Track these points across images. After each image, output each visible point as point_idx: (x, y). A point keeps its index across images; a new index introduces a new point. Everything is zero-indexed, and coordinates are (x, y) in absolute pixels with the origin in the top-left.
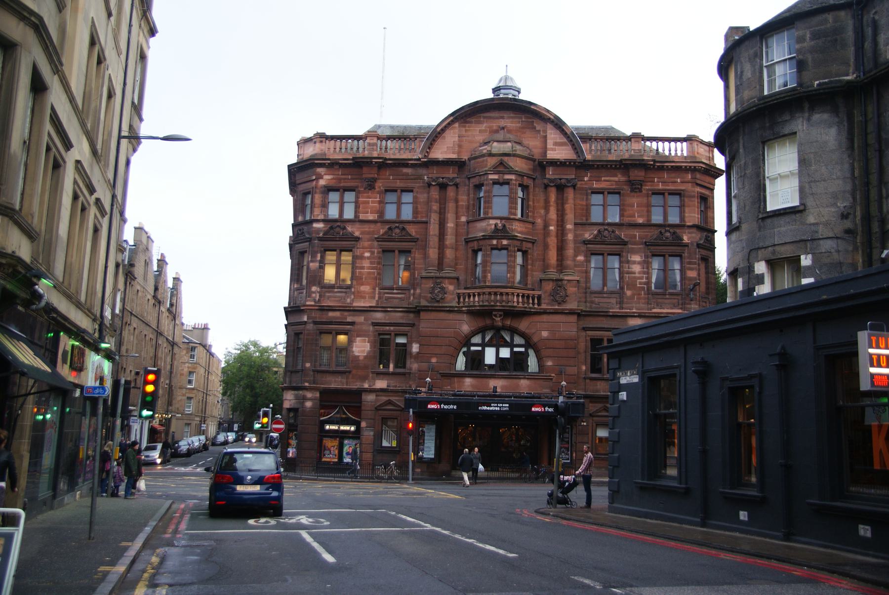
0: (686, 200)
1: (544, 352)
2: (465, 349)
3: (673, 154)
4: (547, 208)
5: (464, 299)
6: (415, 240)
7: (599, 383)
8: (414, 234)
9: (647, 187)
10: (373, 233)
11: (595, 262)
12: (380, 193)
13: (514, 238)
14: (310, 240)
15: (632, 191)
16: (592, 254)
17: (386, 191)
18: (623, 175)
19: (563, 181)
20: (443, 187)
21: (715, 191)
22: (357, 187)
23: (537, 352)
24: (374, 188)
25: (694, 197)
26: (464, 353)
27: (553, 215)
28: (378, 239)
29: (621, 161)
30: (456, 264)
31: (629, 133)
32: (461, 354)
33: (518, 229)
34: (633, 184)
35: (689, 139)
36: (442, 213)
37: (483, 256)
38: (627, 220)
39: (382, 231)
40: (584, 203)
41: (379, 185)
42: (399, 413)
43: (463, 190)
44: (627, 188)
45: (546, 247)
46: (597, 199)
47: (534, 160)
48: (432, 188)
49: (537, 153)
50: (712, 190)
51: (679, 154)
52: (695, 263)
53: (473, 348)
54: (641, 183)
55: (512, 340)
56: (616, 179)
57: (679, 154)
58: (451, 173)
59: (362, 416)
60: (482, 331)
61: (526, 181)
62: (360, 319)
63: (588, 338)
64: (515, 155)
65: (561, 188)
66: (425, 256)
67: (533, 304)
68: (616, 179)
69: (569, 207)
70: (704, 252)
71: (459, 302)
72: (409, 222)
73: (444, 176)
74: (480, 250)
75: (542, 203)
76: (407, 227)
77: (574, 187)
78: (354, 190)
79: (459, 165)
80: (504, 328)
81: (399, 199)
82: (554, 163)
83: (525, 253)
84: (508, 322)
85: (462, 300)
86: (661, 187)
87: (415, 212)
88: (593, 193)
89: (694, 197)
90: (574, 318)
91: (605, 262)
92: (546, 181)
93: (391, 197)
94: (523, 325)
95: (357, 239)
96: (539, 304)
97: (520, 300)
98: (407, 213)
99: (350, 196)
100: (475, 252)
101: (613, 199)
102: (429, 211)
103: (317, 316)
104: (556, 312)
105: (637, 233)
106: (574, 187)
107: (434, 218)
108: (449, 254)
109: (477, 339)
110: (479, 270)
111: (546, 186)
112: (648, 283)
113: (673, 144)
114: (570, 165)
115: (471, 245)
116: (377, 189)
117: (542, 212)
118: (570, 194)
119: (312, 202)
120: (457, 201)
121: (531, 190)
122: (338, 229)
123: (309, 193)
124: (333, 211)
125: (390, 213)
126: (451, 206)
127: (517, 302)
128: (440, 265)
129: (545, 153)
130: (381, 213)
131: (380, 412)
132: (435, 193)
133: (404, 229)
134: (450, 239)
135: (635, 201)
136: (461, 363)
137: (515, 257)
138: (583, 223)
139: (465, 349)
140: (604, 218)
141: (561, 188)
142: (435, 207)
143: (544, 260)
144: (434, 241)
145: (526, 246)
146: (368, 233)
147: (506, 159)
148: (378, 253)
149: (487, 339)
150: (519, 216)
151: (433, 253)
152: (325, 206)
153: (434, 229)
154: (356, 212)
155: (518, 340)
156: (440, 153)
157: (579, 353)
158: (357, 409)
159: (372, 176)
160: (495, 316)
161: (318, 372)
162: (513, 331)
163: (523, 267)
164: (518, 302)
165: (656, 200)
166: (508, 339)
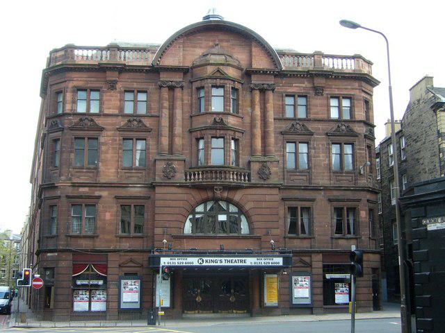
0: (356, 102)
1: (254, 218)
2: (191, 216)
3: (345, 68)
4: (252, 105)
5: (190, 176)
6: (149, 131)
7: (295, 241)
8: (148, 125)
9: (326, 92)
10: (115, 124)
11: (290, 148)
12: (120, 92)
13: (228, 129)
14: (62, 130)
15: (317, 94)
16: (287, 142)
17: (126, 91)
18: (309, 83)
19: (265, 86)
20: (172, 88)
21: (373, 97)
22: (102, 88)
23: (248, 218)
24: (116, 89)
25: (360, 100)
26: (190, 219)
27: (258, 112)
28: (118, 129)
29: (308, 71)
30: (183, 150)
31: (311, 52)
32: (188, 221)
33: (231, 121)
34: (317, 90)
36: (172, 109)
37: (205, 143)
38: (312, 116)
39: (122, 123)
40: (280, 103)
41: (119, 86)
42: (139, 269)
43: (185, 91)
44: (312, 93)
45: (252, 136)
46: (289, 101)
47: (242, 70)
48: (163, 90)
49: (244, 64)
50: (371, 95)
51: (349, 68)
52: (363, 149)
53: (197, 216)
54: (322, 89)
55: (228, 208)
56: (304, 85)
57: (349, 68)
58: (178, 78)
59: (109, 272)
60: (205, 202)
61: (238, 86)
62: (104, 193)
63: (286, 207)
64: (228, 65)
66: (158, 142)
67: (245, 180)
68: (304, 85)
69: (270, 106)
70: (368, 142)
71: (186, 180)
72: (144, 116)
73: (172, 80)
74: (202, 138)
75: (248, 103)
76: (143, 120)
77: (273, 90)
78: (98, 90)
79: (185, 71)
80: (222, 200)
81: (136, 97)
82: (257, 72)
83: (236, 141)
84: (225, 195)
85: (188, 177)
86: (337, 92)
87: (149, 108)
88: (287, 96)
89: (360, 100)
90: (275, 191)
91: (296, 148)
92: (252, 86)
93: (129, 96)
94: (237, 196)
95: (102, 129)
96: (249, 180)
97: (235, 177)
98: (142, 110)
99: (95, 95)
100: (198, 140)
101: (302, 101)
102: (161, 108)
103: (70, 191)
104: (262, 187)
105: (320, 126)
106: (273, 90)
107: (166, 113)
108: (178, 141)
109: (200, 209)
110: (201, 154)
111: (252, 90)
112: (330, 164)
113: (344, 60)
114: (270, 74)
115: (194, 134)
116: (118, 90)
117: (249, 109)
118: (270, 96)
119: (64, 99)
120: (182, 100)
121: (240, 92)
122: (86, 121)
123: (61, 92)
124: (81, 108)
125: (129, 109)
126: (178, 103)
127: (232, 179)
128: (171, 151)
129: (251, 64)
130: (121, 109)
131: (124, 269)
132: (165, 93)
133: (140, 121)
134: (178, 130)
135: (317, 101)
136: (188, 228)
137: (230, 143)
138: (281, 119)
139: (191, 216)
140: (295, 115)
141: (263, 91)
142: (166, 104)
143: (251, 146)
144: (165, 131)
145: (238, 135)
146: (112, 124)
147: (221, 67)
148: (119, 140)
149: (208, 208)
150: (232, 112)
151: (165, 141)
152: (74, 102)
153: (165, 122)
154: (101, 108)
155: (233, 209)
156: (169, 61)
157: (280, 218)
158: (104, 268)
159: (114, 79)
160: (216, 189)
161: (71, 237)
162: (229, 201)
163: (237, 152)
164: (233, 179)
165: (334, 102)
166: (225, 207)
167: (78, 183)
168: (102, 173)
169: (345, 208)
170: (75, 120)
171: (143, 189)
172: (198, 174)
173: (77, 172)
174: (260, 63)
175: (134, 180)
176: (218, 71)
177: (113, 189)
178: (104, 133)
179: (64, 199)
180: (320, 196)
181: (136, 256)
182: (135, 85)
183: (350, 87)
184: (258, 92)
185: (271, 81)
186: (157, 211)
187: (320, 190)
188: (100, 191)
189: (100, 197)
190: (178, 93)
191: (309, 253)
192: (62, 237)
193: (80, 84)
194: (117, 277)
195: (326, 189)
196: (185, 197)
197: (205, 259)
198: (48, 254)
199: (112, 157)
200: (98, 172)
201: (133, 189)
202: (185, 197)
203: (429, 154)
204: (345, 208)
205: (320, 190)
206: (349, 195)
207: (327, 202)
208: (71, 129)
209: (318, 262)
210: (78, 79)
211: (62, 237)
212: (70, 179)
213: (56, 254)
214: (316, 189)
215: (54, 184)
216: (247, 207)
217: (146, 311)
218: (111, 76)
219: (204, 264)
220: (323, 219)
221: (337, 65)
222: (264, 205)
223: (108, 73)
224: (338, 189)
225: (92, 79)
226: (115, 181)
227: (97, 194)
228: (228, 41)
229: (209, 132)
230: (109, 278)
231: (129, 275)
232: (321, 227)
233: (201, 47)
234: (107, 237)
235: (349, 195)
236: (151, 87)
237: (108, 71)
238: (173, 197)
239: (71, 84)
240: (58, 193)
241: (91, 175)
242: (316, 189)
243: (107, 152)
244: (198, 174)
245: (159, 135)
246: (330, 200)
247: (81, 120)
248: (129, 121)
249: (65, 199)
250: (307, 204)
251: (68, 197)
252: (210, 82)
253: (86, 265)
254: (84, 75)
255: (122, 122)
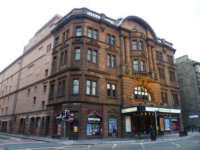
20: (125, 38)
27: (151, 54)
35: (171, 44)
41: (105, 31)
58: (126, 34)
62: (101, 76)
65: (152, 47)
76: (115, 47)
94: (149, 85)
95: (99, 47)
103: (87, 73)
116: (105, 33)
122: (94, 42)
124: (90, 36)
131: (109, 113)
132: (122, 38)
142: (123, 43)
146: (103, 46)
152: (88, 32)
158: (101, 112)
159: (104, 27)
167: (91, 69)
168: (100, 67)
170: (89, 40)
171: (117, 77)
172: (137, 74)
173: (89, 64)
174: (150, 36)
175: (112, 72)
176: (141, 36)
177: (104, 75)
178: (100, 49)
179: (84, 76)
180: (168, 89)
181: (115, 108)
182: (111, 33)
184: (150, 47)
185: (153, 44)
186: (124, 87)
187: (169, 87)
188: (99, 75)
189: (99, 78)
190: (127, 40)
192: (83, 95)
193: (90, 25)
194: (107, 117)
195: (170, 87)
196: (133, 83)
197: (160, 109)
198: (74, 104)
199: (103, 60)
200: (98, 66)
201: (112, 76)
202: (133, 83)
203: (190, 80)
205: (169, 87)
208: (87, 44)
210: (89, 23)
211: (83, 95)
212: (87, 67)
213: (80, 104)
214: (168, 86)
215: (79, 68)
216: (153, 90)
217: (120, 134)
218: (103, 26)
221: (167, 44)
222: (157, 90)
223: (102, 25)
224: (173, 87)
225: (95, 25)
226: (106, 71)
227: (98, 76)
228: (139, 27)
229: (140, 57)
230: (104, 117)
231: (113, 116)
233: (131, 26)
234: (102, 97)
236: (117, 36)
237: (102, 22)
238: (130, 82)
239: (86, 25)
240: (80, 73)
241: (95, 67)
242: (168, 86)
243: (101, 58)
244: (137, 74)
245: (121, 56)
246: (171, 91)
247: (92, 41)
248: (110, 47)
249: (84, 76)
251: (86, 75)
252: (138, 39)
253: (93, 110)
254: (92, 22)
255: (108, 47)
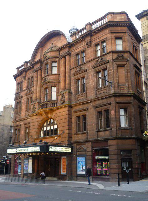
56: (83, 45)
68: (83, 45)
169: (103, 111)
180: (90, 106)
183: (104, 35)
191: (84, 143)
195: (92, 101)
197: (18, 149)
204: (103, 111)
205: (90, 102)
206: (105, 101)
207: (93, 109)
209: (88, 147)
214: (87, 103)
219: (18, 152)
220: (92, 120)
232: (91, 125)
235: (105, 101)
250: (84, 113)
